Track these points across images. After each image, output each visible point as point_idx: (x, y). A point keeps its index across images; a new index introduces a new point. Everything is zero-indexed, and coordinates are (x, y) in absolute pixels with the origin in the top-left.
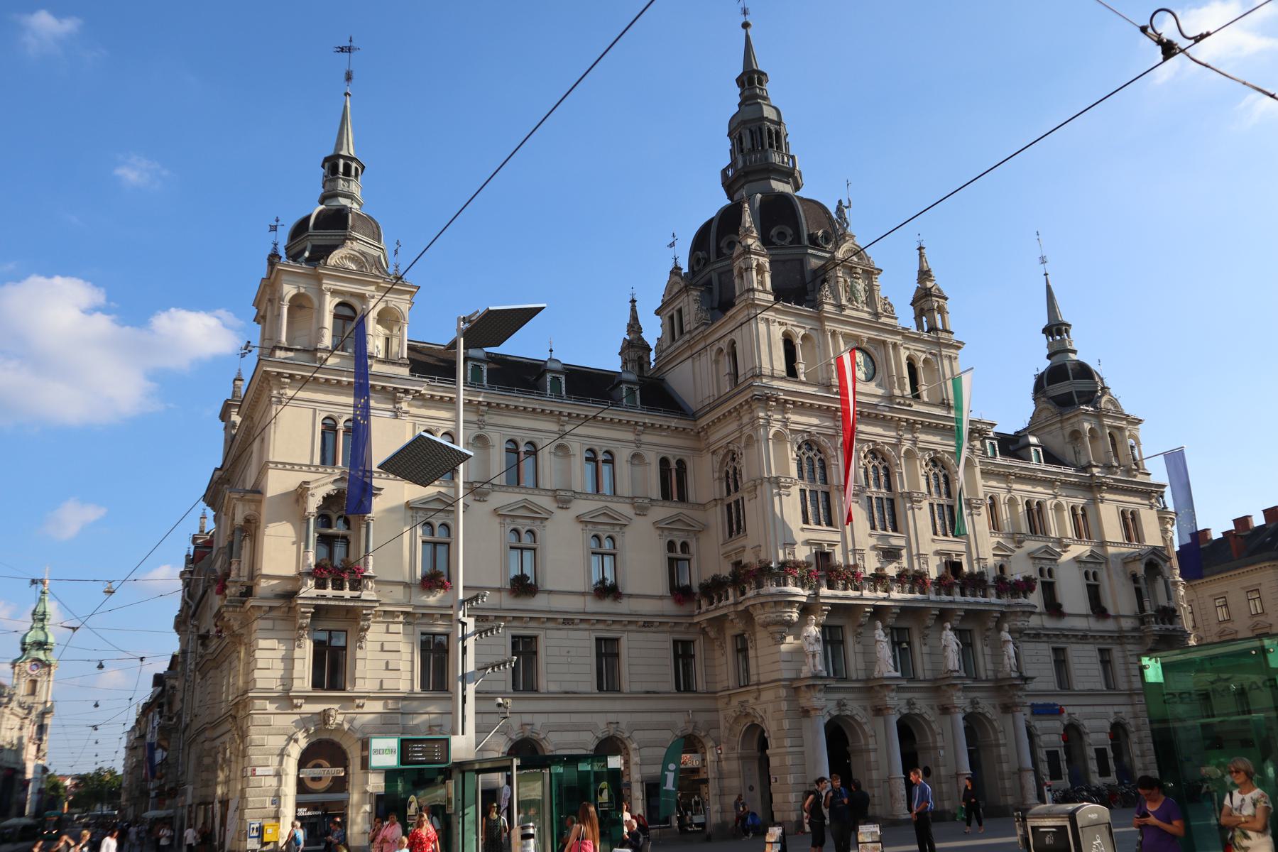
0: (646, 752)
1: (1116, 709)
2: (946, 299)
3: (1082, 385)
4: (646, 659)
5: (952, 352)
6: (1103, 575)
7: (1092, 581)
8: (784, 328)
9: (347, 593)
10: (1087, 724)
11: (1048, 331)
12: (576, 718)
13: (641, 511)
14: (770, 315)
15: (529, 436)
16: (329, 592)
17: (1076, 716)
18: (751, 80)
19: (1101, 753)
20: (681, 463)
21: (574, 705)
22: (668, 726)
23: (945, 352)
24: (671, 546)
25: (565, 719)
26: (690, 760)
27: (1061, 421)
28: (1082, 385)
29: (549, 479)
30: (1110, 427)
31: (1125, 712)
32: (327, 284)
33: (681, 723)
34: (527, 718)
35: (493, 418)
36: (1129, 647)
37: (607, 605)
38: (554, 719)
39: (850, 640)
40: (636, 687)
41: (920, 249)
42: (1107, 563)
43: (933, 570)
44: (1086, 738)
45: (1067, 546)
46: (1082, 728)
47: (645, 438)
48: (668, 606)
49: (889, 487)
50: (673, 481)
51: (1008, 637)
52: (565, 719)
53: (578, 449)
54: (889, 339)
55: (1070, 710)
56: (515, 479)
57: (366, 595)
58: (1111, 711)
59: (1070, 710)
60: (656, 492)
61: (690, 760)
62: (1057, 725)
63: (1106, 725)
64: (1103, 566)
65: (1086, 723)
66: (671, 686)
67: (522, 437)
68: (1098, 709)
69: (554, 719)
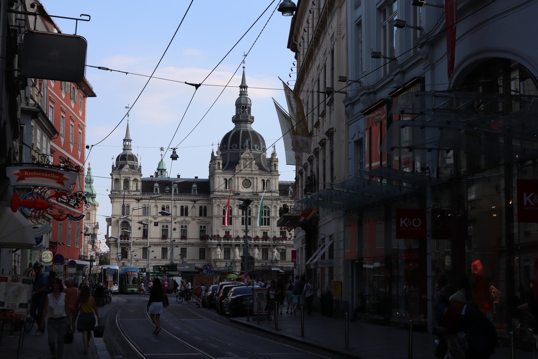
5: (276, 177)
9: (126, 241)
13: (193, 220)
14: (220, 175)
15: (167, 204)
16: (123, 241)
18: (243, 86)
20: (205, 207)
23: (274, 177)
24: (201, 227)
32: (122, 176)
37: (184, 241)
39: (231, 251)
43: (260, 235)
48: (199, 241)
50: (203, 212)
54: (255, 177)
57: (130, 241)
60: (198, 214)
66: (198, 258)
67: (166, 205)
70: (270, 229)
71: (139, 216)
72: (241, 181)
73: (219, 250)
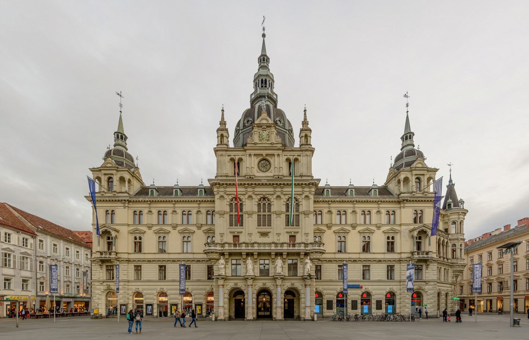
1: (391, 287)
4: (198, 271)
6: (397, 238)
10: (373, 292)
17: (370, 289)
25: (173, 287)
26: (210, 298)
31: (395, 288)
33: (208, 288)
34: (162, 287)
35: (153, 205)
36: (402, 264)
38: (169, 287)
40: (194, 279)
42: (400, 233)
44: (373, 297)
45: (380, 227)
46: (371, 293)
47: (201, 205)
53: (179, 211)
55: (367, 287)
59: (367, 287)
61: (210, 298)
62: (359, 292)
63: (385, 293)
64: (399, 234)
65: (374, 292)
68: (380, 287)
71: (128, 225)
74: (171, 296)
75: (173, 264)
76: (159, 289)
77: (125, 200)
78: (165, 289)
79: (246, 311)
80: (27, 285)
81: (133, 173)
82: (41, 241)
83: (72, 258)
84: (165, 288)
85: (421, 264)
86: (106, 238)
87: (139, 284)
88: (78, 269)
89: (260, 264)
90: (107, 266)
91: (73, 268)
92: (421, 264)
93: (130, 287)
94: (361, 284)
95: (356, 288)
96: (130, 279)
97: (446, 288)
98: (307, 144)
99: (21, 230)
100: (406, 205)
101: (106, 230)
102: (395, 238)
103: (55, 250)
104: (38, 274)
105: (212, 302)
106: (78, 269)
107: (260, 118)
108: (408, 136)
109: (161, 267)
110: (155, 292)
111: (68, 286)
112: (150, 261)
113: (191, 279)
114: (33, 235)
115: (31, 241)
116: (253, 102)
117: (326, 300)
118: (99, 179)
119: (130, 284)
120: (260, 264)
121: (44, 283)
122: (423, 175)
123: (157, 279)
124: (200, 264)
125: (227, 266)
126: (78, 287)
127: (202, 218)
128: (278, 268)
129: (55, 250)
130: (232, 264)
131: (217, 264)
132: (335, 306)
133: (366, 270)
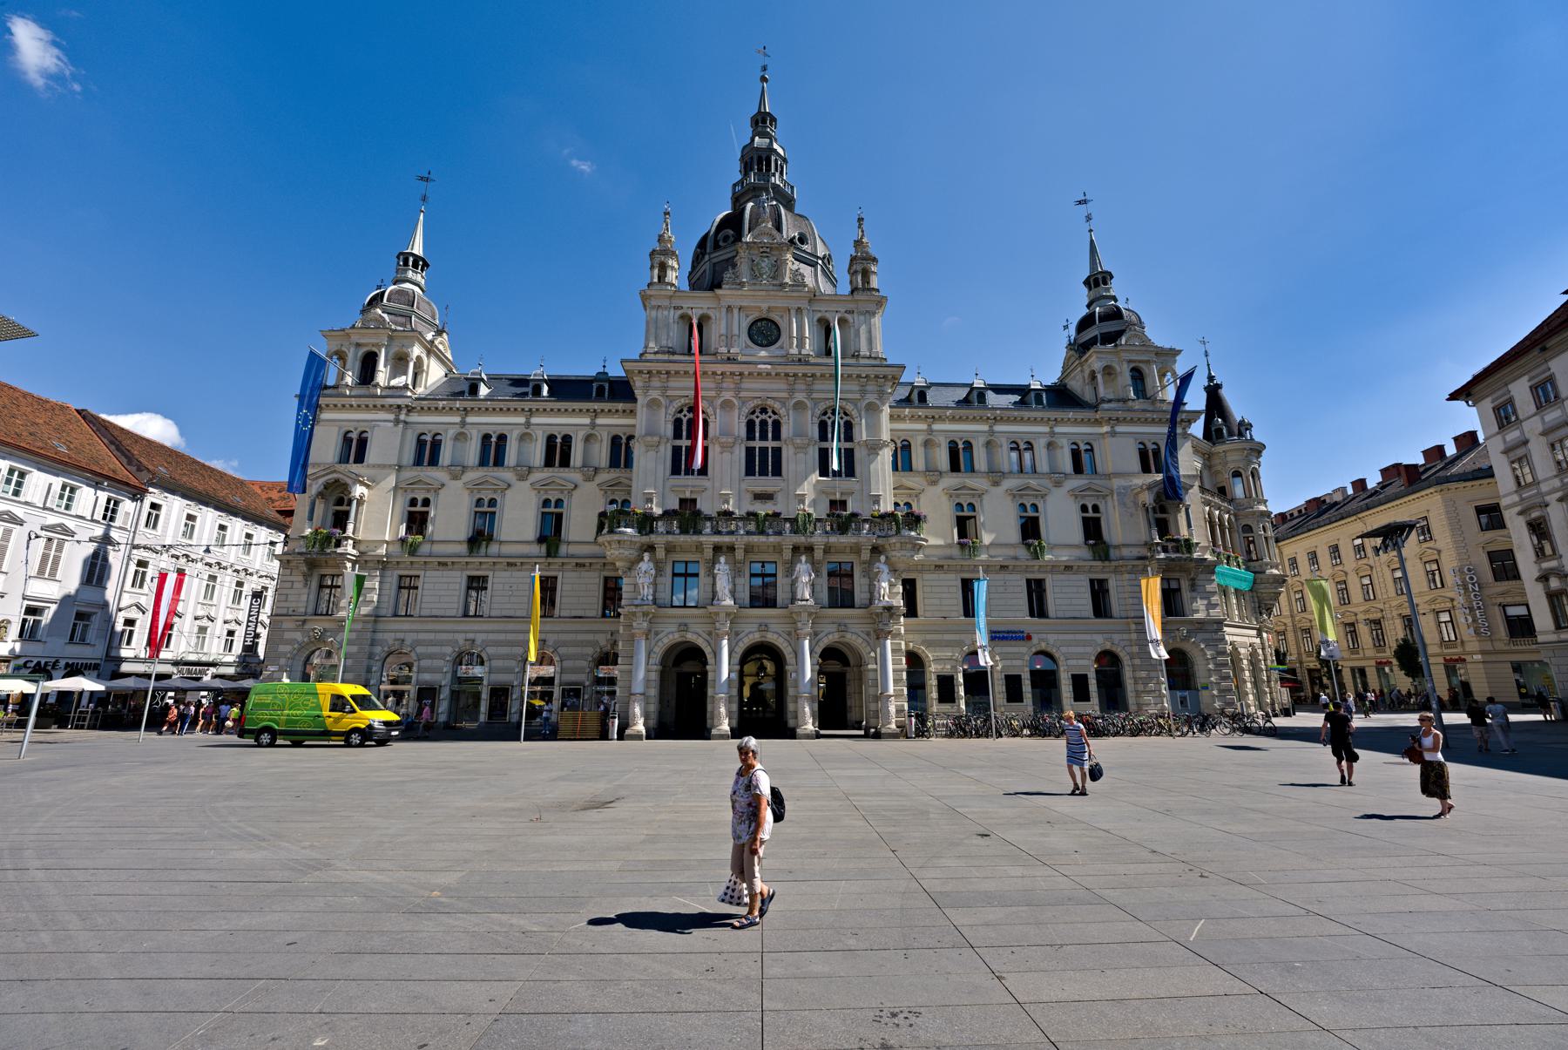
0: (567, 664)
2: (875, 260)
3: (1111, 327)
7: (1091, 514)
8: (679, 312)
11: (1087, 283)
12: (510, 637)
13: (589, 479)
15: (500, 430)
19: (1080, 683)
21: (511, 626)
22: (594, 644)
27: (1081, 364)
28: (1111, 327)
29: (511, 456)
30: (1130, 361)
33: (603, 640)
34: (471, 636)
41: (860, 220)
49: (777, 437)
51: (885, 569)
52: (502, 637)
56: (483, 462)
58: (1099, 638)
69: (492, 637)
70: (857, 487)
72: (741, 324)
73: (646, 565)
74: (495, 663)
75: (507, 574)
76: (461, 642)
77: (399, 407)
78: (478, 642)
79: (709, 708)
80: (86, 626)
81: (432, 342)
82: (154, 506)
83: (232, 555)
84: (480, 638)
85: (1177, 575)
86: (333, 499)
87: (406, 626)
88: (240, 584)
89: (752, 575)
90: (323, 576)
91: (227, 582)
92: (1177, 575)
93: (379, 636)
94: (1027, 629)
95: (1016, 639)
96: (383, 612)
97: (1245, 639)
98: (867, 288)
99: (108, 478)
100: (1119, 429)
101: (337, 481)
102: (1102, 508)
103: (189, 531)
104: (125, 596)
105: (612, 681)
106: (240, 584)
107: (756, 231)
108: (1098, 280)
109: (471, 579)
110: (448, 650)
111: (203, 630)
112: (445, 564)
113: (557, 612)
114: (137, 494)
115: (127, 506)
116: (738, 201)
117: (934, 677)
118: (341, 356)
119: (381, 626)
120: (752, 575)
121: (138, 623)
122: (1148, 362)
123: (460, 613)
124: (585, 574)
125: (659, 580)
126: (231, 633)
127: (602, 453)
128: (800, 587)
129: (189, 531)
130: (675, 575)
131: (634, 573)
132: (962, 693)
133: (1036, 591)
